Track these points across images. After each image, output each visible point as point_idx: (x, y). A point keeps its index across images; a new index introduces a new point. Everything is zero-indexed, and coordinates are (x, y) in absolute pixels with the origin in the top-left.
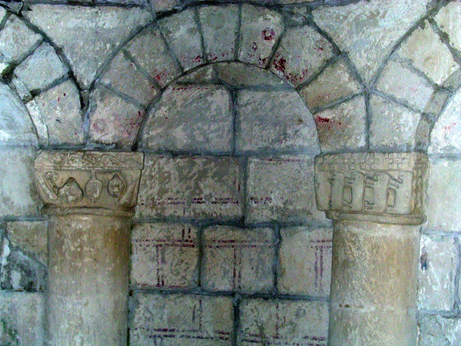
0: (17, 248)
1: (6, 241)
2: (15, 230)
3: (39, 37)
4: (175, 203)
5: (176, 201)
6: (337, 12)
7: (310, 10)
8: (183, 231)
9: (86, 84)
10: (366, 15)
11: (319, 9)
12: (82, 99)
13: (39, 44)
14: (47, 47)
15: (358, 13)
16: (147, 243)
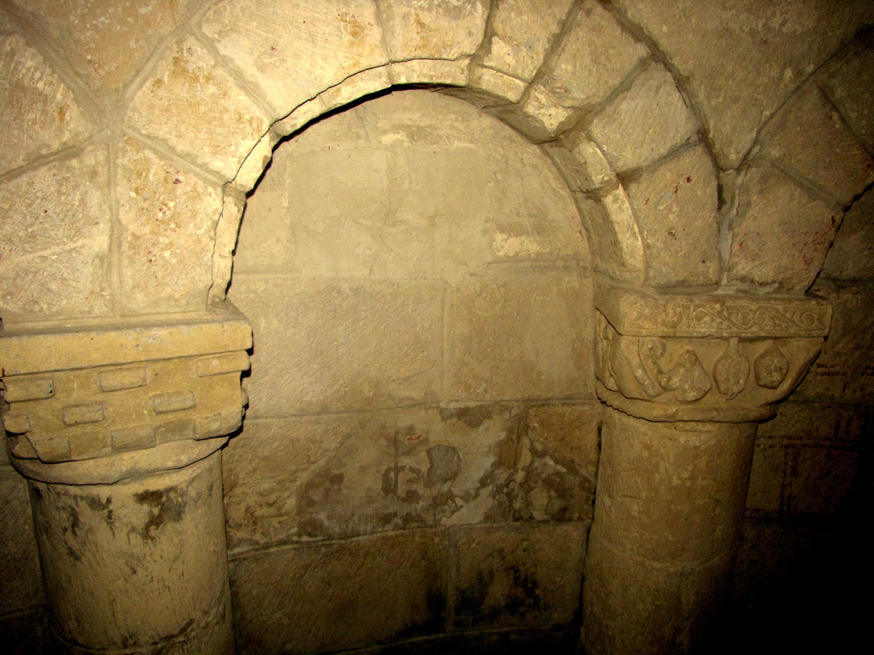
0: (543, 454)
1: (525, 441)
2: (542, 423)
3: (642, 50)
4: (828, 374)
5: (831, 370)
8: (838, 424)
9: (733, 157)
12: (720, 190)
13: (643, 65)
14: (658, 75)
16: (770, 442)
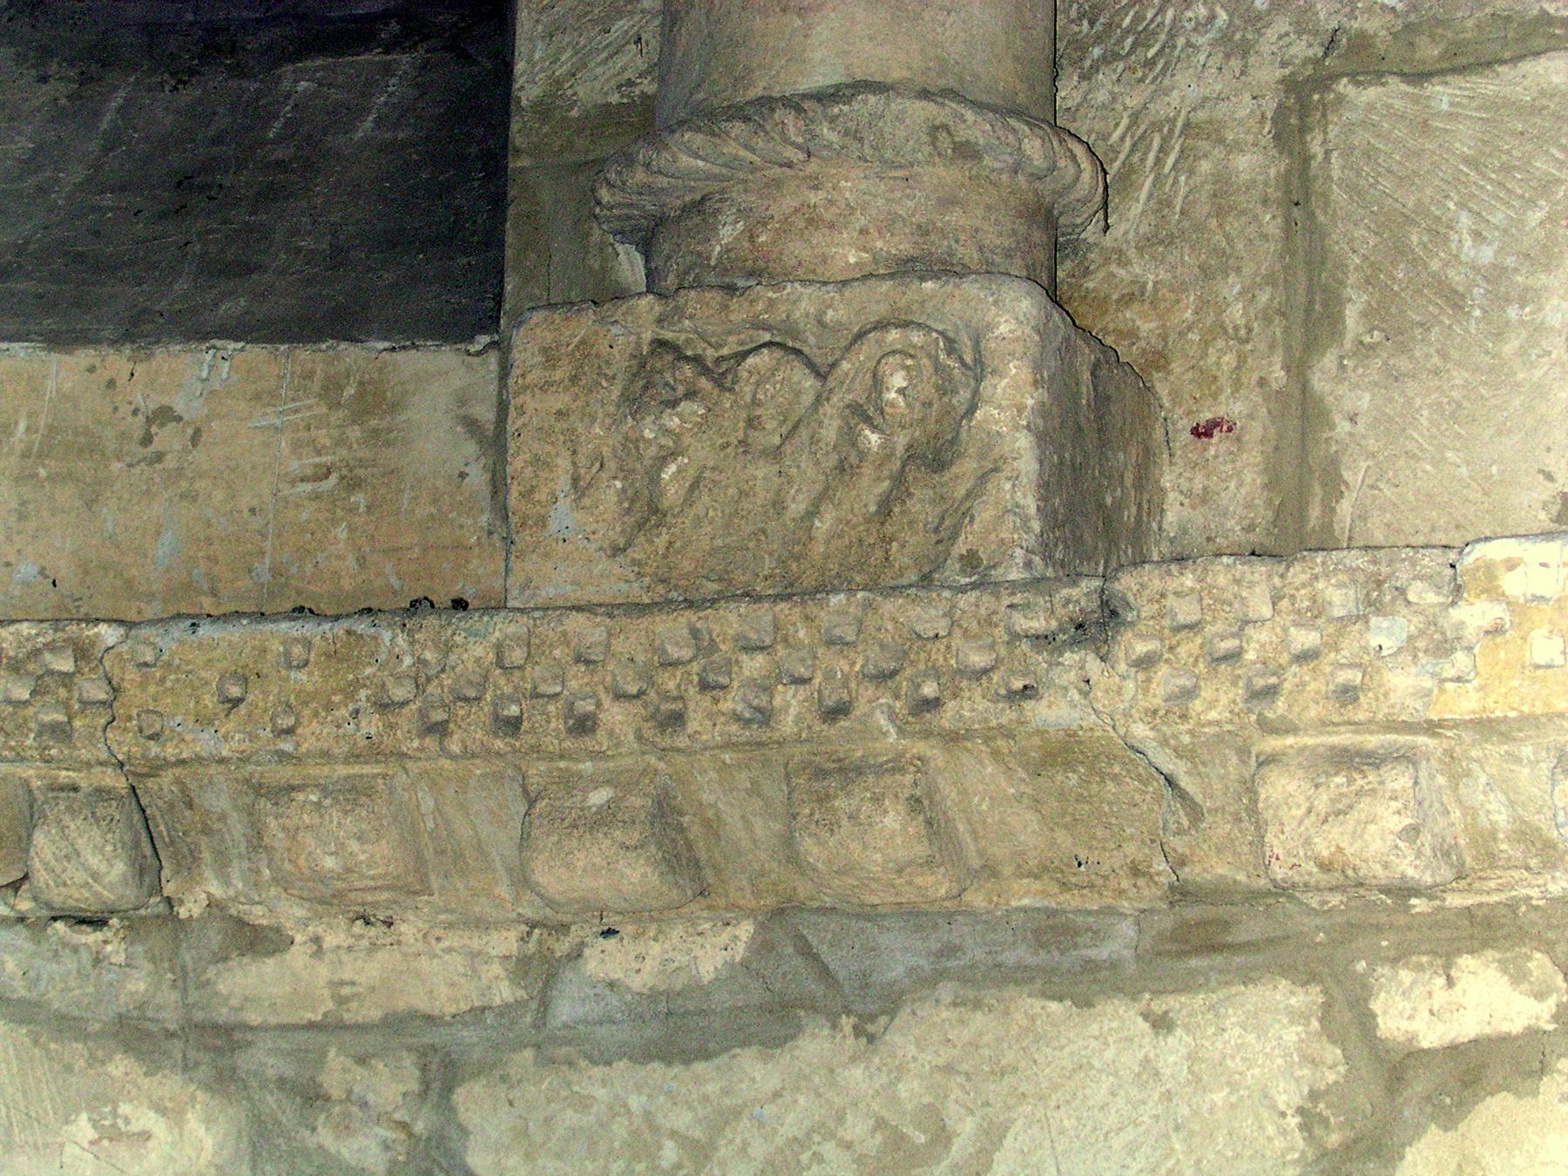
6: (636, 1102)
7: (442, 1075)
10: (848, 1146)
11: (504, 1079)
15: (791, 1126)
